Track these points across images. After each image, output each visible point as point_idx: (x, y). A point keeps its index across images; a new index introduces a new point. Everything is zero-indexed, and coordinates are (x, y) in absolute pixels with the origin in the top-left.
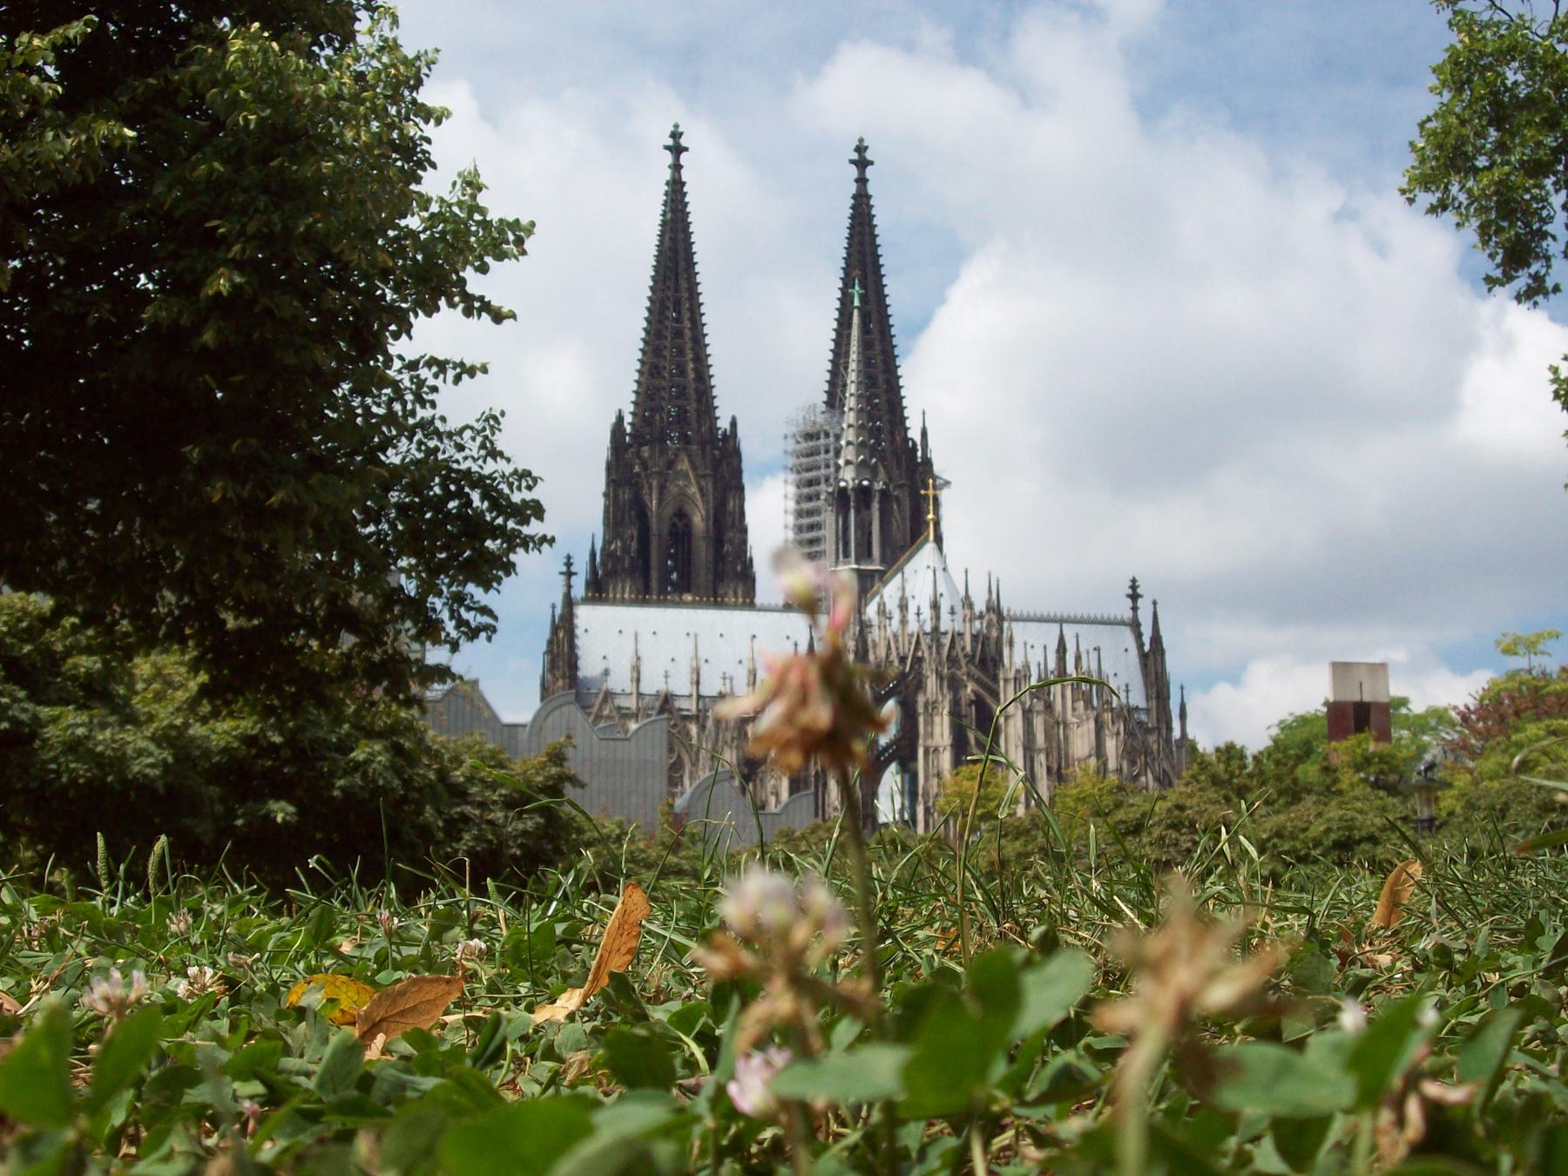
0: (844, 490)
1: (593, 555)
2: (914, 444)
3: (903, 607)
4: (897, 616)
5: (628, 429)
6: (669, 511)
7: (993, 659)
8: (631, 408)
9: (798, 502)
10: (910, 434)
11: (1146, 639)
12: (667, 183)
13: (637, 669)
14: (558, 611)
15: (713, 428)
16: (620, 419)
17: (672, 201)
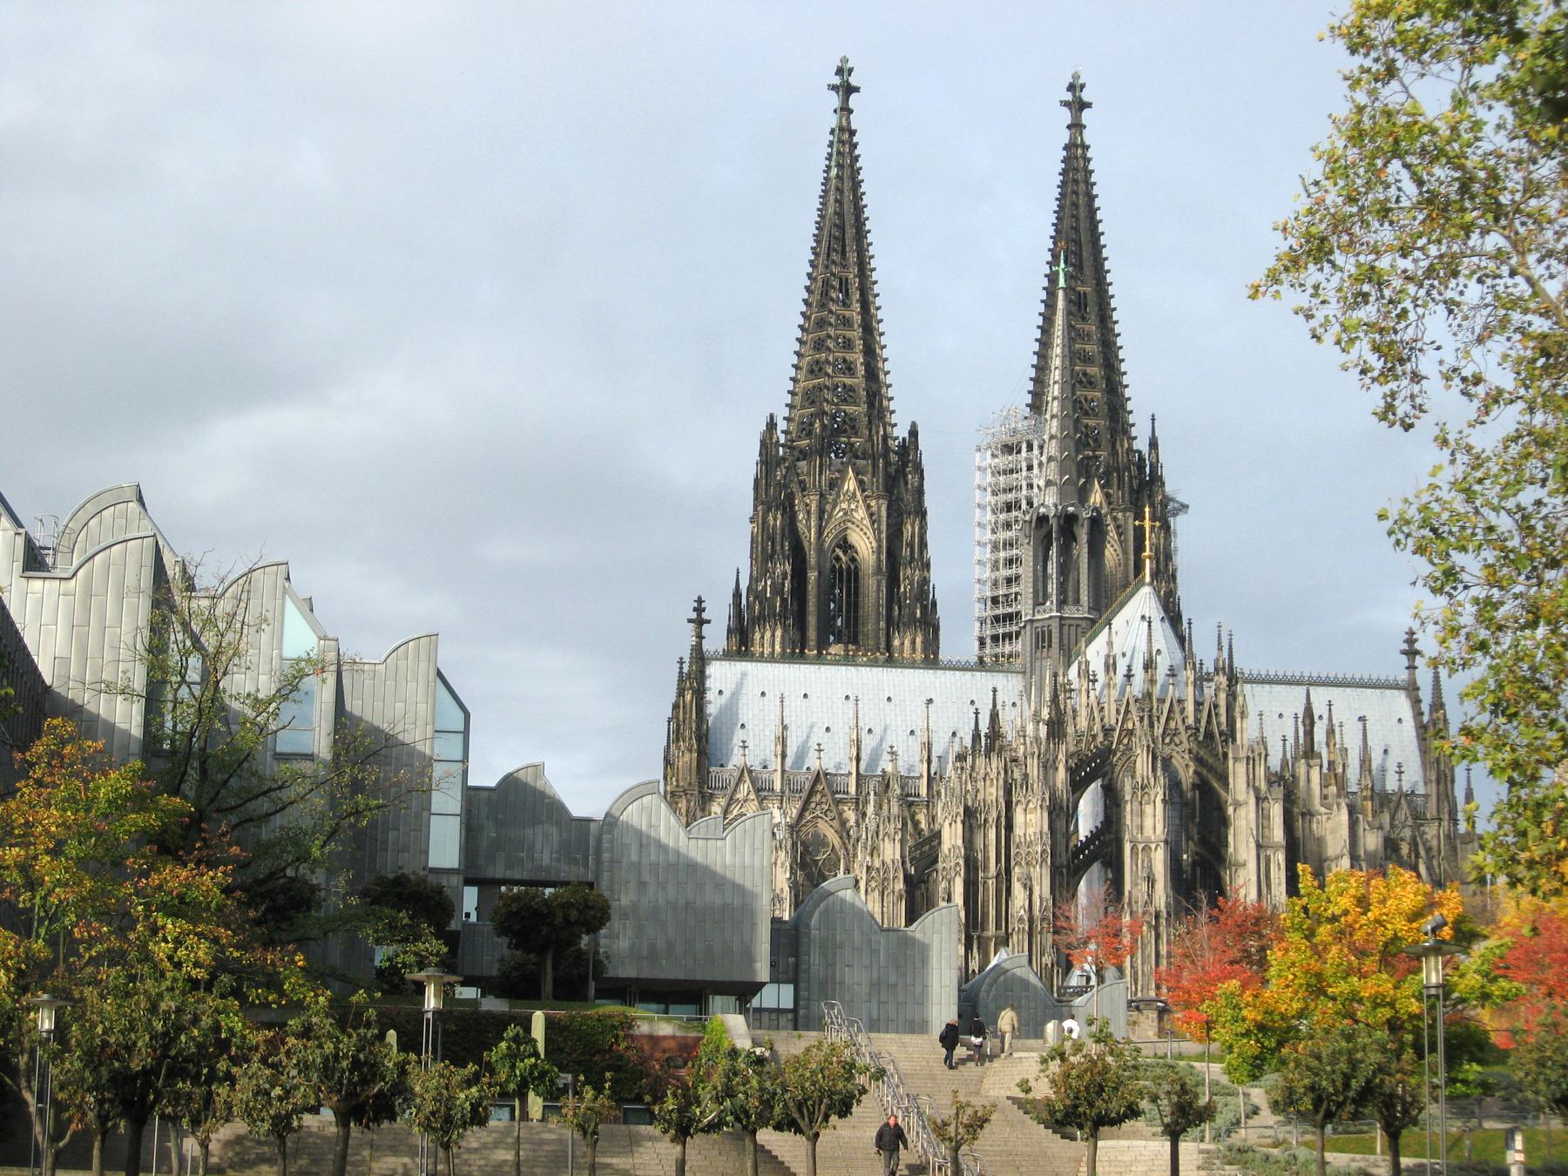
0: (1042, 520)
1: (737, 595)
2: (1141, 459)
3: (1110, 666)
11: (1425, 707)
14: (686, 669)
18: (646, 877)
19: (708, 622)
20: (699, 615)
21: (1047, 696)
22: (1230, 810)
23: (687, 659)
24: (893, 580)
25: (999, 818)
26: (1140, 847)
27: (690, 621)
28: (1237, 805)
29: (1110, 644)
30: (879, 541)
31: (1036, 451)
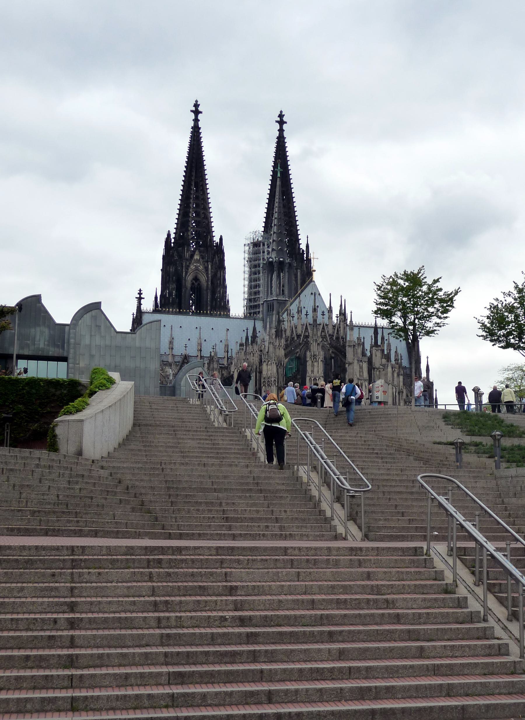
0: (272, 262)
1: (156, 298)
2: (303, 251)
3: (299, 311)
4: (296, 316)
5: (173, 241)
6: (190, 278)
7: (342, 338)
8: (175, 231)
9: (250, 275)
10: (301, 247)
12: (192, 128)
13: (171, 343)
14: (135, 316)
15: (212, 241)
16: (169, 235)
17: (194, 135)
18: (93, 352)
19: (144, 298)
20: (140, 296)
21: (274, 324)
22: (347, 366)
23: (135, 313)
24: (214, 293)
25: (256, 368)
26: (312, 379)
27: (136, 298)
28: (350, 364)
29: (300, 303)
30: (208, 277)
31: (266, 246)
